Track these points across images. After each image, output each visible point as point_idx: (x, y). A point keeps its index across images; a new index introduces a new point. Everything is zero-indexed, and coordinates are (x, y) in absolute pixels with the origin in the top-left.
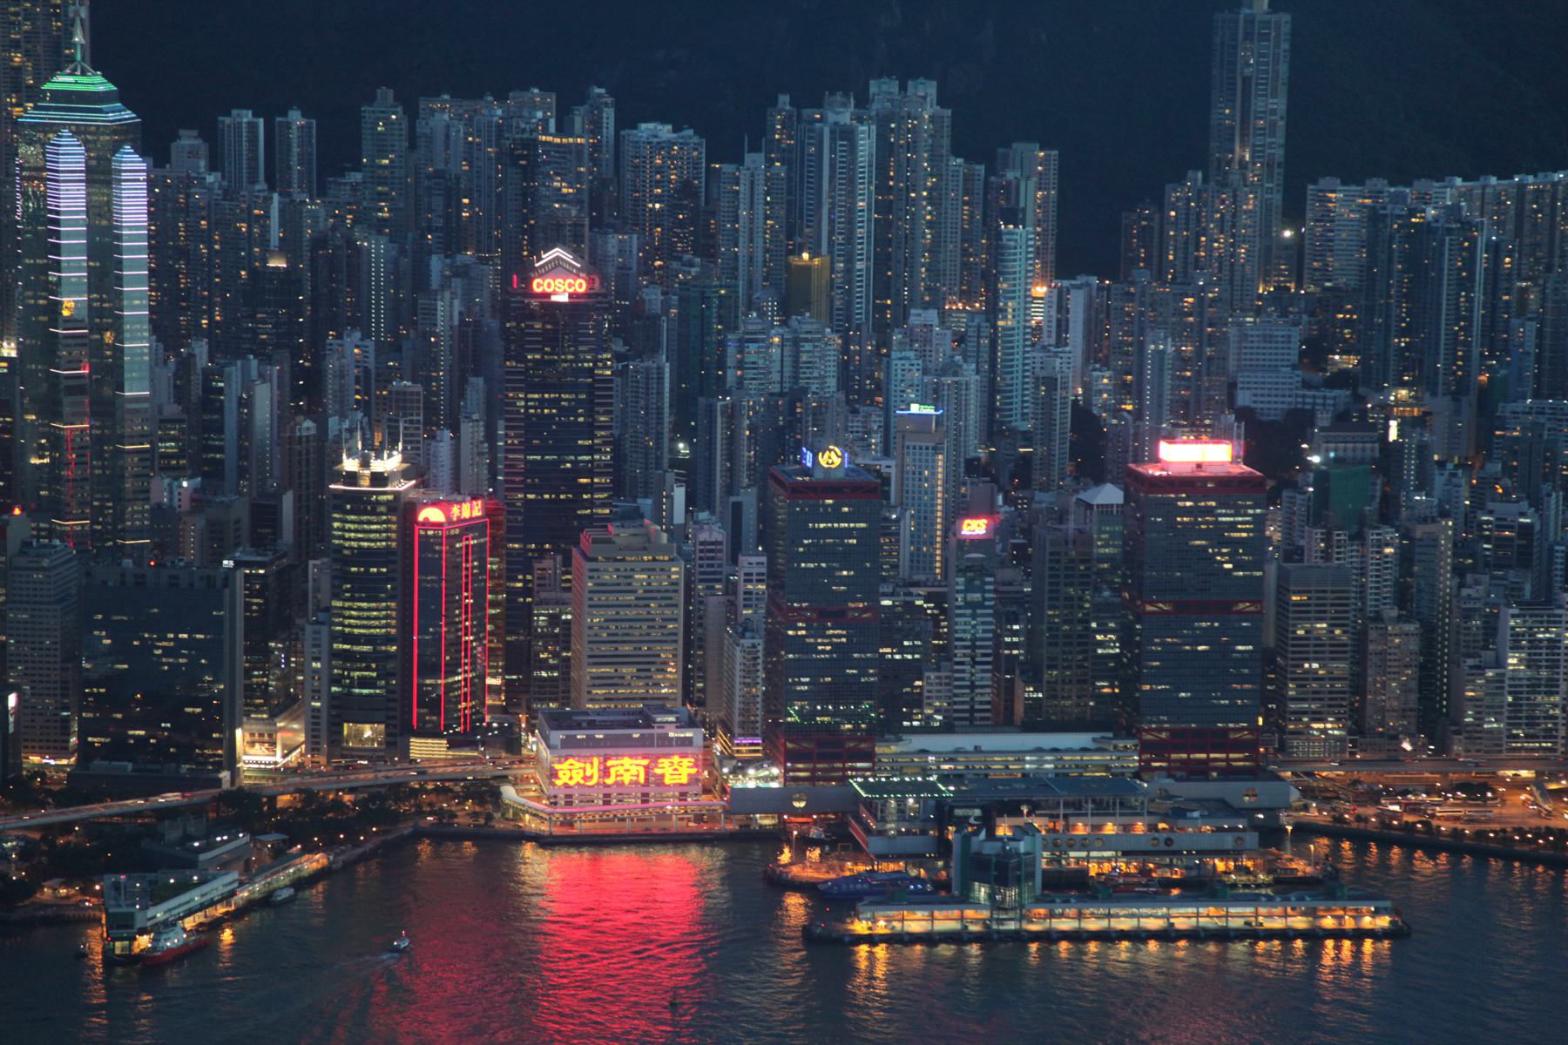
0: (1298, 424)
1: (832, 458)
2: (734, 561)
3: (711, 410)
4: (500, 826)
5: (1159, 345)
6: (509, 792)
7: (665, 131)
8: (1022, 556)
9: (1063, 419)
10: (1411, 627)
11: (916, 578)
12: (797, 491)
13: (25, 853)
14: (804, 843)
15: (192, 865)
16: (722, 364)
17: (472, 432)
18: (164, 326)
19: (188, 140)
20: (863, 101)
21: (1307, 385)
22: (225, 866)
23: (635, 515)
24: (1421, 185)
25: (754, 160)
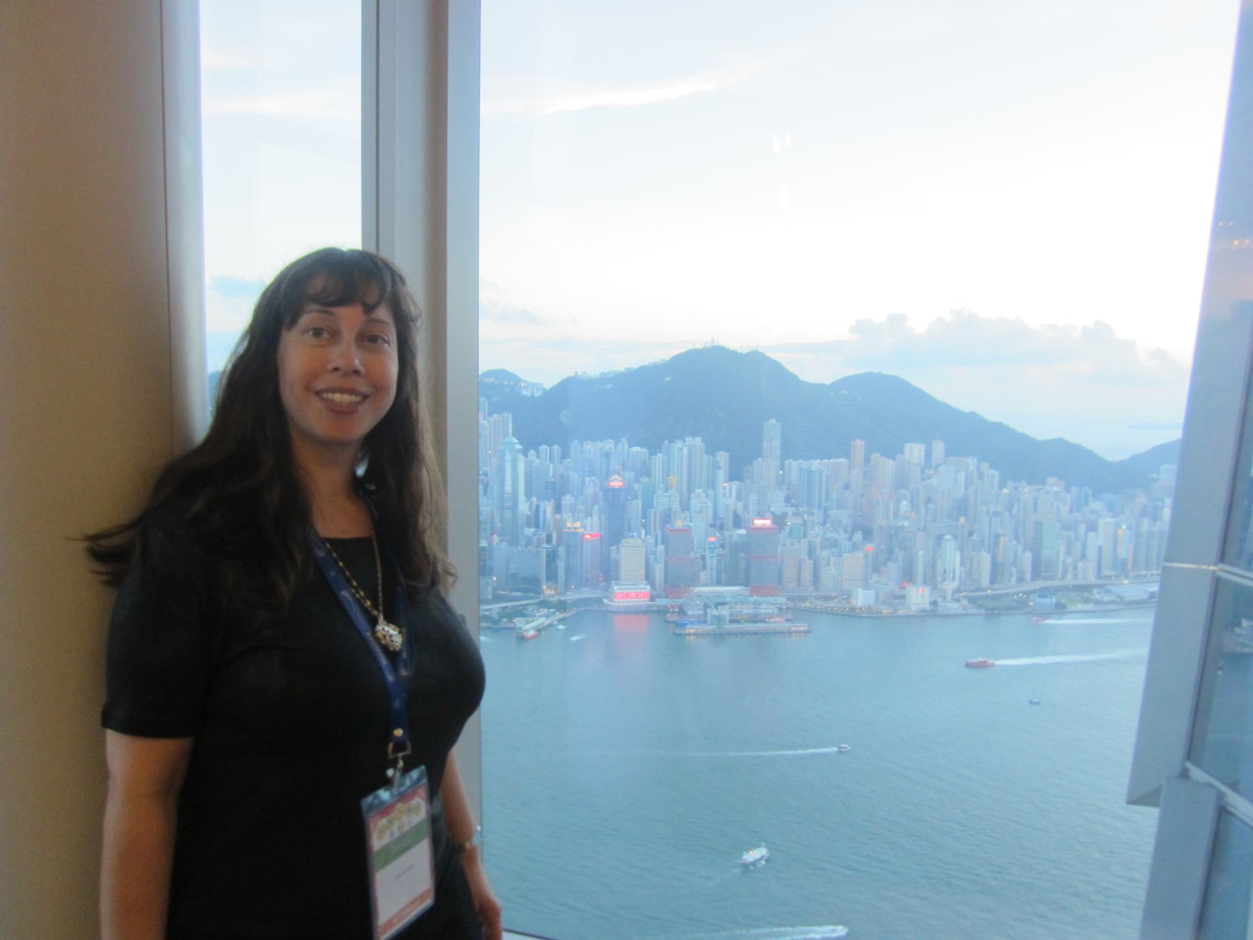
0: (785, 515)
1: (679, 524)
2: (656, 547)
3: (650, 513)
4: (603, 609)
5: (753, 497)
6: (605, 601)
7: (639, 449)
8: (722, 546)
9: (731, 514)
10: (811, 561)
11: (699, 551)
12: (671, 531)
13: (498, 613)
14: (674, 612)
15: (535, 616)
16: (652, 504)
17: (595, 517)
18: (528, 495)
19: (532, 452)
20: (684, 442)
21: (786, 506)
22: (542, 616)
23: (633, 537)
24: (811, 461)
25: (660, 455)
